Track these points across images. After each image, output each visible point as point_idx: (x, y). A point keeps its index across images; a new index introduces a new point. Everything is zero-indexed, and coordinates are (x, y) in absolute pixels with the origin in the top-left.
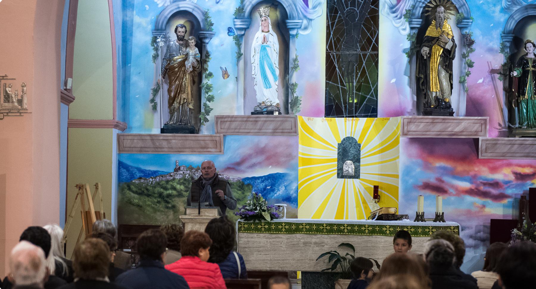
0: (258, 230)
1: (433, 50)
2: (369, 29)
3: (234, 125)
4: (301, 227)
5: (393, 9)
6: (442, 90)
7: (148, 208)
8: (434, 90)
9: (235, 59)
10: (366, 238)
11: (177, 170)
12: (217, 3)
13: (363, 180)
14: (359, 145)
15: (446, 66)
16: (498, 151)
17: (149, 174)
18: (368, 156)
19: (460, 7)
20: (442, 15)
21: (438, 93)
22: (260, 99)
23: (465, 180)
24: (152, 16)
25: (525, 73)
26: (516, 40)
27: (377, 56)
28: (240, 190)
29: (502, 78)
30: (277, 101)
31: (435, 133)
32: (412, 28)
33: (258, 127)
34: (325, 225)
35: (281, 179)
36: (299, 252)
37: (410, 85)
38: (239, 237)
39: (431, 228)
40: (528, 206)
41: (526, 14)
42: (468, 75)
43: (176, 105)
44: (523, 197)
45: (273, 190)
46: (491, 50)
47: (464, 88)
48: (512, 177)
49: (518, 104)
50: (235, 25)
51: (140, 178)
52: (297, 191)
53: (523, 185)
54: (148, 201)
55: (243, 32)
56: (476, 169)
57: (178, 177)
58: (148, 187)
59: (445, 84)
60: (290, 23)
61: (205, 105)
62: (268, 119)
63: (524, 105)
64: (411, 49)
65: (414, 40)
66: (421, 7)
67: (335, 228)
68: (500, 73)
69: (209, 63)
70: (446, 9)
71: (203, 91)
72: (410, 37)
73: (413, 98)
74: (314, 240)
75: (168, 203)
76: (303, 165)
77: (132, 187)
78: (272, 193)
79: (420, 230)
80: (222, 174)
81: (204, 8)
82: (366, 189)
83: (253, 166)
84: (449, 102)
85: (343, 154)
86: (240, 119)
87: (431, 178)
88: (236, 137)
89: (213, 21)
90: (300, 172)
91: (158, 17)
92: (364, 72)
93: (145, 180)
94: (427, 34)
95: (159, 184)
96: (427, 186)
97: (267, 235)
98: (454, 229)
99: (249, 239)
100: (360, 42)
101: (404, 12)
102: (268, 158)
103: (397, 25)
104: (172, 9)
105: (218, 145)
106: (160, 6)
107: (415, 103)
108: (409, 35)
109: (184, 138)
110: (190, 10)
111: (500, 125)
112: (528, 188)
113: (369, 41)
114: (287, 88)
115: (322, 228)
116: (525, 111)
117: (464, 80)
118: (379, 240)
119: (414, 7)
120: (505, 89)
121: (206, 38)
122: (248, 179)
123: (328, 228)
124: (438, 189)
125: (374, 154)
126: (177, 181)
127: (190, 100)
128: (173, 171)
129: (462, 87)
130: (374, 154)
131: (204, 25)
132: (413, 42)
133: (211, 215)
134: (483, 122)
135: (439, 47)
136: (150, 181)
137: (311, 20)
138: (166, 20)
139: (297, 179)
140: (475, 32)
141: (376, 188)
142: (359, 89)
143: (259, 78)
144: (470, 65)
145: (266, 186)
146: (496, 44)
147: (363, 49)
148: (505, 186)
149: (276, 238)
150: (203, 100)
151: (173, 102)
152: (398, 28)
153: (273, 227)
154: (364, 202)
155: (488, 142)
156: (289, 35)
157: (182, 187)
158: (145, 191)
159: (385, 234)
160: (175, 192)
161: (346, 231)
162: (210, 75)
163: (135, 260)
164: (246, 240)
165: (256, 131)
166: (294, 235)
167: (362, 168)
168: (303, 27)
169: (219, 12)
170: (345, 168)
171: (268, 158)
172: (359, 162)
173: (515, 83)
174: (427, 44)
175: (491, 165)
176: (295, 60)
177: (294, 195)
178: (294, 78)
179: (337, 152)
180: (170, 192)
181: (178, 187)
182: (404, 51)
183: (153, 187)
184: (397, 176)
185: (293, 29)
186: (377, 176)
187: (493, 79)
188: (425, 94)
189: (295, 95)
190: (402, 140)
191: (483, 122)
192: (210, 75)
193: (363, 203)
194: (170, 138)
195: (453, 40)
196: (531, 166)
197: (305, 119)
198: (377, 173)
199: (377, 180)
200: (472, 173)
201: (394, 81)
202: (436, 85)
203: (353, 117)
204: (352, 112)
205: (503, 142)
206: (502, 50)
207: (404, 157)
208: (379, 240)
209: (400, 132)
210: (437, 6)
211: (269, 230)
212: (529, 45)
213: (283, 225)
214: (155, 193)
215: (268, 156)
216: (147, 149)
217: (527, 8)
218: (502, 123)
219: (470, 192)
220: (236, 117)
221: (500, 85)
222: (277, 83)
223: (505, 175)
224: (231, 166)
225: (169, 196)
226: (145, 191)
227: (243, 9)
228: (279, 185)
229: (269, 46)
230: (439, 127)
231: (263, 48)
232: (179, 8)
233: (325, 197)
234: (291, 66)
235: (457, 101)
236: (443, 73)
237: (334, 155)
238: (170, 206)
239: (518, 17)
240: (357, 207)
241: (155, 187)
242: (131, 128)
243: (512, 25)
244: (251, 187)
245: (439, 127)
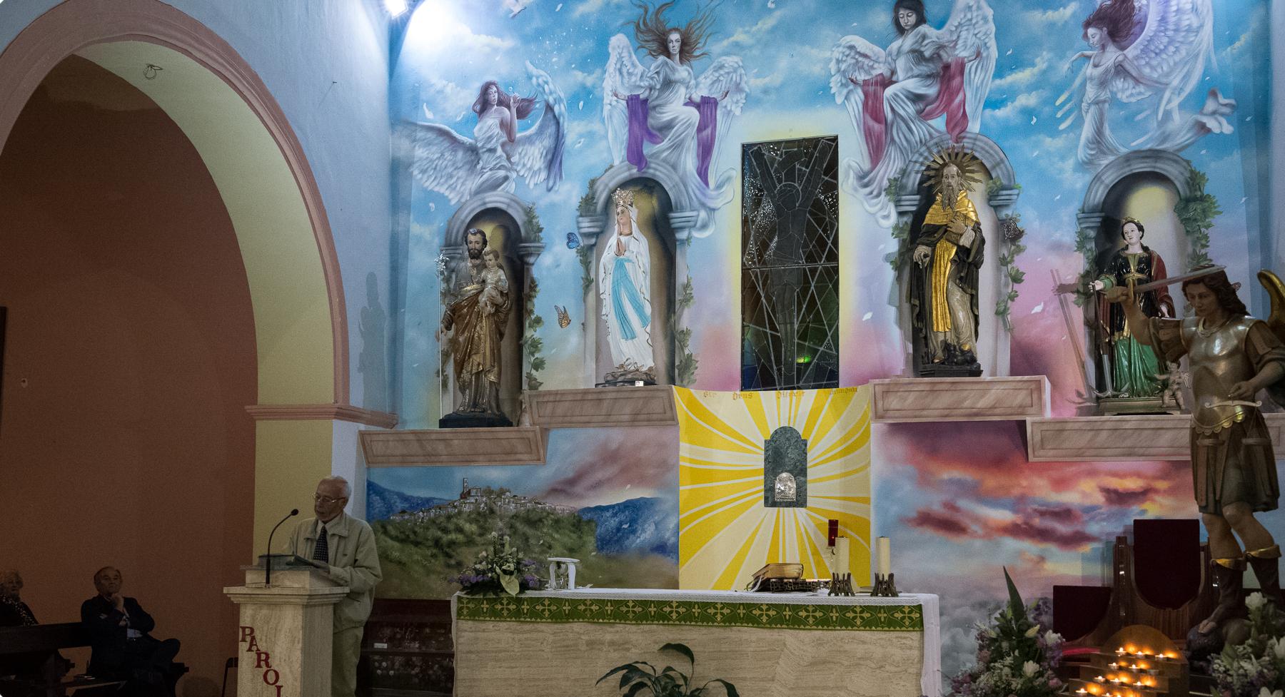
0: (496, 615)
1: (938, 251)
2: (820, 221)
3: (561, 409)
4: (582, 607)
5: (864, 179)
6: (956, 328)
8: (941, 329)
9: (581, 291)
10: (717, 632)
11: (466, 495)
12: (549, 190)
14: (805, 443)
15: (961, 278)
16: (1066, 445)
18: (822, 463)
19: (994, 167)
20: (953, 182)
21: (948, 335)
22: (617, 360)
23: (1004, 506)
24: (440, 223)
25: (1121, 282)
26: (1107, 222)
27: (836, 270)
29: (1081, 301)
30: (650, 363)
31: (936, 412)
32: (901, 214)
33: (604, 412)
34: (631, 604)
36: (579, 662)
37: (900, 322)
38: (458, 630)
39: (858, 610)
40: (1132, 559)
41: (1127, 171)
42: (1012, 298)
43: (465, 375)
44: (1120, 540)
45: (633, 532)
46: (1057, 247)
47: (1004, 321)
48: (1099, 499)
49: (1111, 349)
50: (579, 228)
51: (403, 512)
53: (1124, 515)
54: (416, 554)
55: (593, 241)
56: (1024, 483)
57: (466, 509)
58: (417, 529)
59: (962, 316)
60: (676, 218)
61: (529, 376)
62: (619, 395)
63: (1122, 351)
64: (901, 254)
65: (905, 236)
66: (917, 172)
67: (653, 609)
68: (1078, 292)
69: (535, 300)
70: (963, 170)
71: (526, 351)
72: (897, 230)
73: (905, 348)
74: (608, 637)
75: (450, 557)
76: (693, 483)
77: (390, 528)
79: (834, 615)
81: (527, 200)
82: (818, 526)
83: (597, 486)
84: (970, 351)
85: (775, 461)
86: (570, 398)
87: (934, 502)
88: (568, 432)
89: (542, 222)
90: (682, 497)
91: (449, 222)
92: (812, 303)
94: (929, 220)
96: (926, 519)
97: (514, 625)
98: (910, 612)
99: (480, 635)
100: (806, 246)
101: (885, 183)
102: (624, 470)
103: (873, 210)
104: (474, 207)
105: (536, 449)
106: (453, 202)
107: (911, 357)
108: (896, 227)
109: (472, 436)
110: (503, 207)
111: (1079, 395)
112: (1130, 522)
113: (822, 243)
114: (673, 338)
115: (624, 609)
116: (1126, 363)
117: (1006, 309)
118: (745, 636)
119: (904, 172)
120: (1087, 323)
121: (530, 255)
122: (589, 510)
123: (638, 609)
124: (949, 525)
125: (833, 458)
126: (465, 516)
127: (488, 367)
129: (1001, 323)
130: (833, 458)
131: (527, 232)
132: (904, 241)
133: (296, 585)
134: (1033, 386)
135: (950, 245)
137: (714, 210)
138: (465, 225)
139: (676, 509)
140: (1026, 214)
141: (833, 525)
142: (803, 337)
143: (612, 322)
144: (1017, 279)
145: (621, 523)
146: (1067, 233)
147: (810, 258)
148: (1086, 518)
149: (530, 631)
150: (526, 368)
151: (461, 372)
152: (873, 215)
153: (525, 607)
154: (816, 553)
155: (1045, 427)
156: (675, 240)
157: (474, 528)
158: (412, 536)
159: (759, 623)
160: (460, 537)
161: (674, 615)
162: (538, 321)
163: (393, 664)
164: (472, 635)
165: (600, 418)
166: (567, 626)
167: (809, 486)
168: (699, 224)
169: (553, 206)
170: (778, 486)
171: (624, 470)
172: (805, 475)
173: (1104, 311)
174: (924, 239)
175: (1054, 474)
176: (687, 286)
177: (673, 540)
178: (686, 320)
179: (763, 457)
180: (453, 536)
182: (887, 258)
184: (866, 500)
185: (682, 228)
186: (838, 502)
187: (1063, 304)
188: (926, 338)
189: (687, 352)
190: (876, 428)
191: (1033, 386)
192: (538, 321)
194: (448, 436)
195: (977, 228)
196: (1139, 475)
197: (697, 394)
198: (838, 495)
199: (837, 509)
200: (1016, 492)
201: (868, 316)
202: (944, 318)
203: (793, 388)
204: (794, 380)
205: (1076, 426)
206: (1081, 246)
207: (881, 460)
208: (745, 636)
209: (870, 414)
210: (945, 165)
211: (517, 615)
212: (1129, 228)
213: (547, 602)
215: (622, 464)
216: (416, 459)
217: (1128, 158)
218: (1083, 391)
219: (1015, 530)
220: (563, 393)
221: (1078, 314)
222: (648, 329)
223: (1084, 494)
225: (452, 544)
226: (412, 536)
227: (593, 198)
229: (629, 261)
230: (945, 400)
231: (620, 266)
232: (485, 203)
233: (726, 541)
234: (678, 297)
235: (990, 349)
236: (958, 296)
237: (757, 461)
239: (1110, 178)
242: (404, 422)
243: (1099, 194)
245: (945, 400)
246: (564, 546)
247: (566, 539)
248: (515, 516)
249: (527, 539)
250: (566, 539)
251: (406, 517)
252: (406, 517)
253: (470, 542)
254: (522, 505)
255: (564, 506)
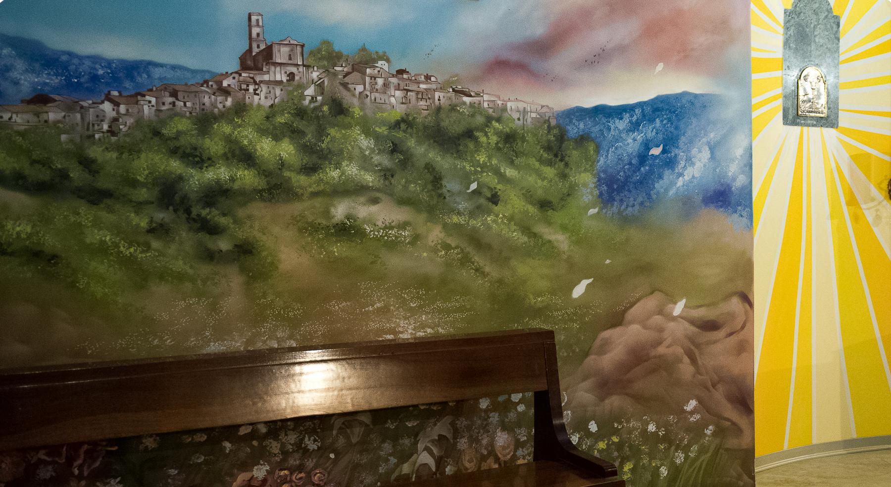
7: (100, 267)
11: (256, 60)
13: (849, 132)
17: (95, 78)
28: (550, 163)
35: (695, 115)
45: (670, 163)
51: (41, 99)
52: (749, 166)
57: (261, 99)
58: (95, 152)
78: (667, 174)
80: (473, 88)
83: (598, 60)
93: (70, 108)
95: (157, 133)
122: (581, 113)
126: (257, 117)
128: (233, 65)
136: (100, 118)
145: (647, 145)
154: (852, 201)
157: (287, 150)
160: (246, 177)
177: (741, 181)
181: (265, 147)
183: (120, 149)
193: (849, 204)
214: (134, 183)
224: (514, 57)
225: (216, 194)
228: (691, 142)
238: (224, 245)
240: (832, 217)
241: (131, 149)
244: (591, 147)
246: (528, 195)
247: (531, 180)
248: (405, 123)
249: (436, 180)
250: (531, 180)
251: (53, 115)
252: (52, 116)
253: (276, 188)
254: (421, 95)
255: (525, 102)
